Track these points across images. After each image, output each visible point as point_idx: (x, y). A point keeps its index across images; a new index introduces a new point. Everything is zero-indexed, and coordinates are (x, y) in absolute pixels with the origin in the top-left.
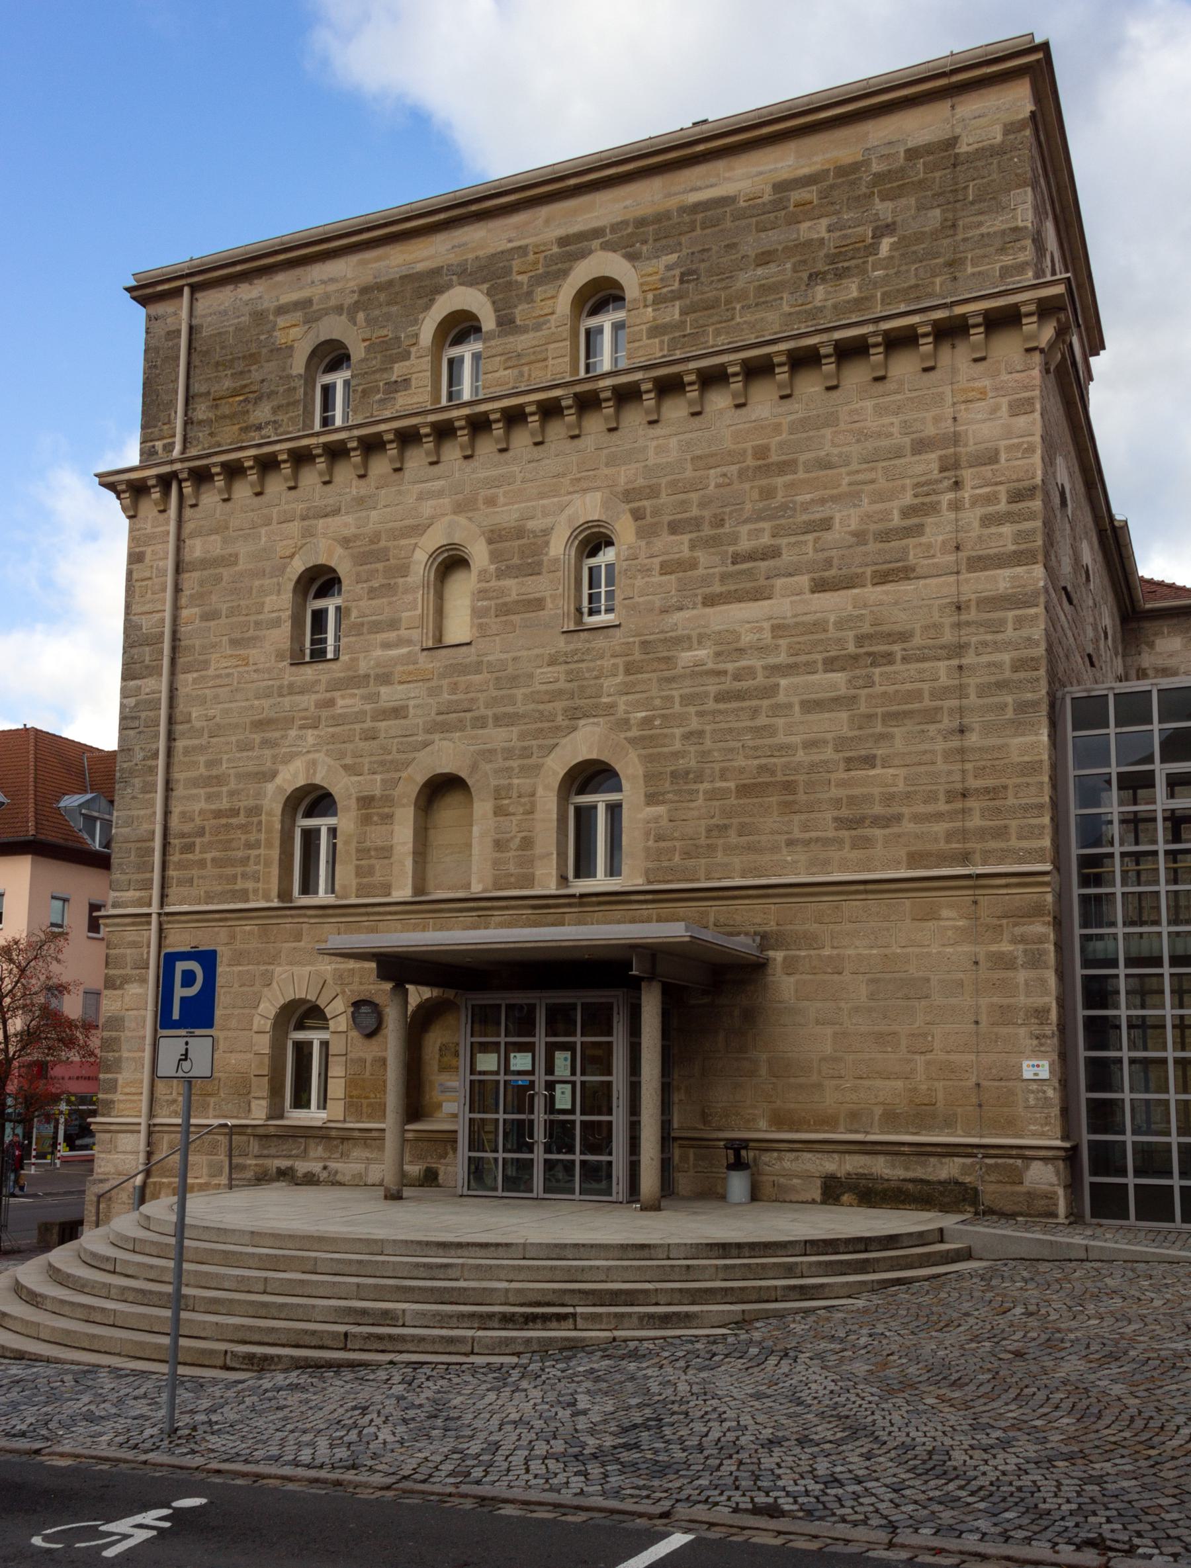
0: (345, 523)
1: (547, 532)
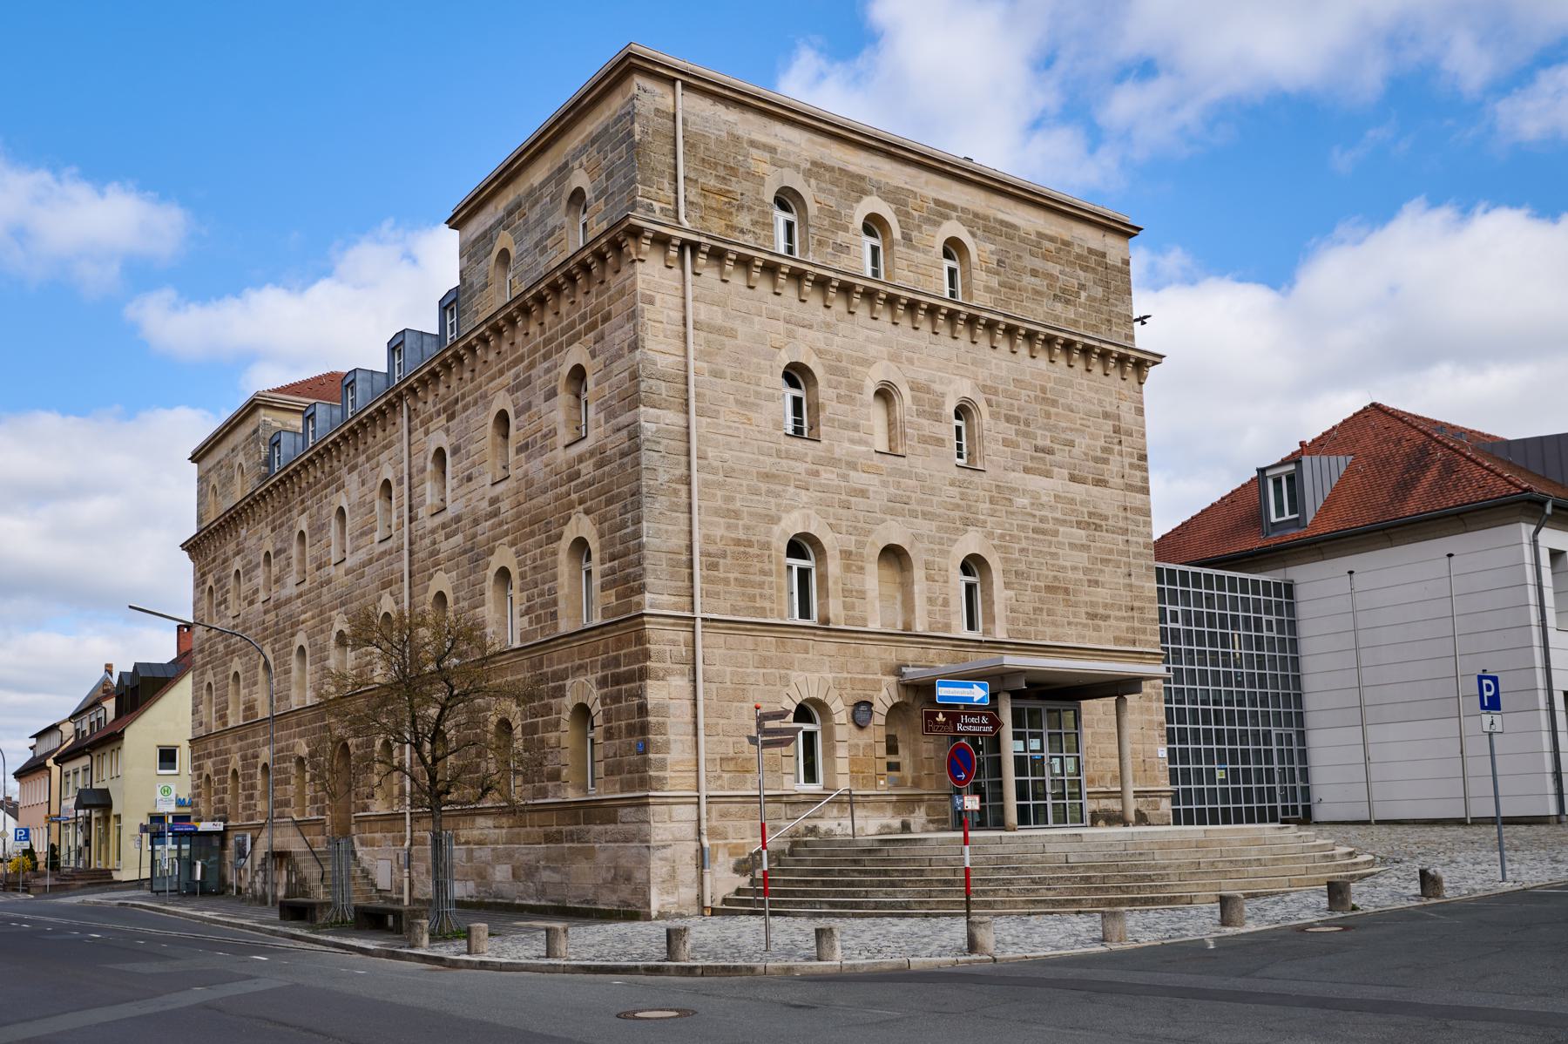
1: (943, 395)
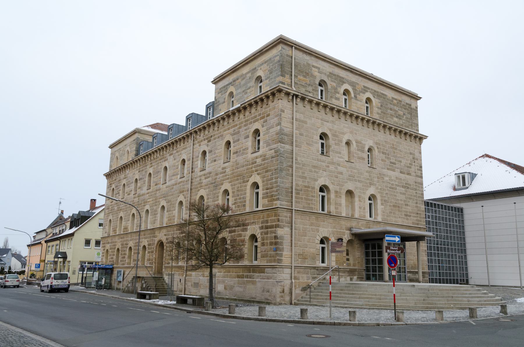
1: (365, 145)
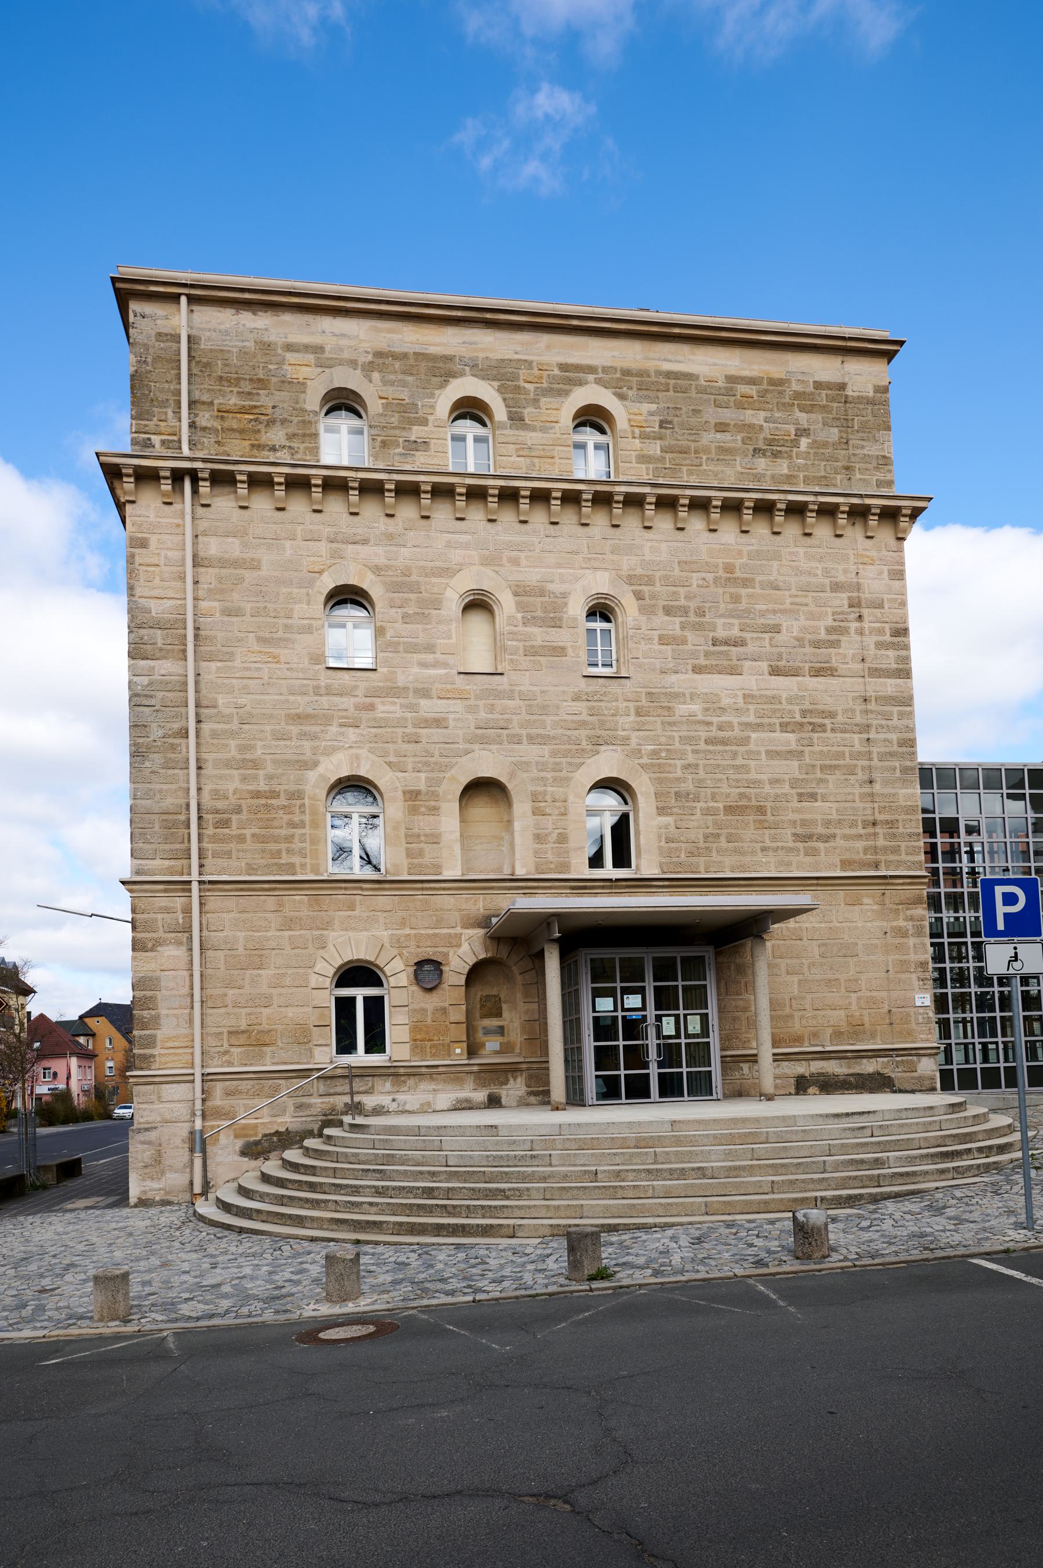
0: (377, 553)
1: (564, 595)
